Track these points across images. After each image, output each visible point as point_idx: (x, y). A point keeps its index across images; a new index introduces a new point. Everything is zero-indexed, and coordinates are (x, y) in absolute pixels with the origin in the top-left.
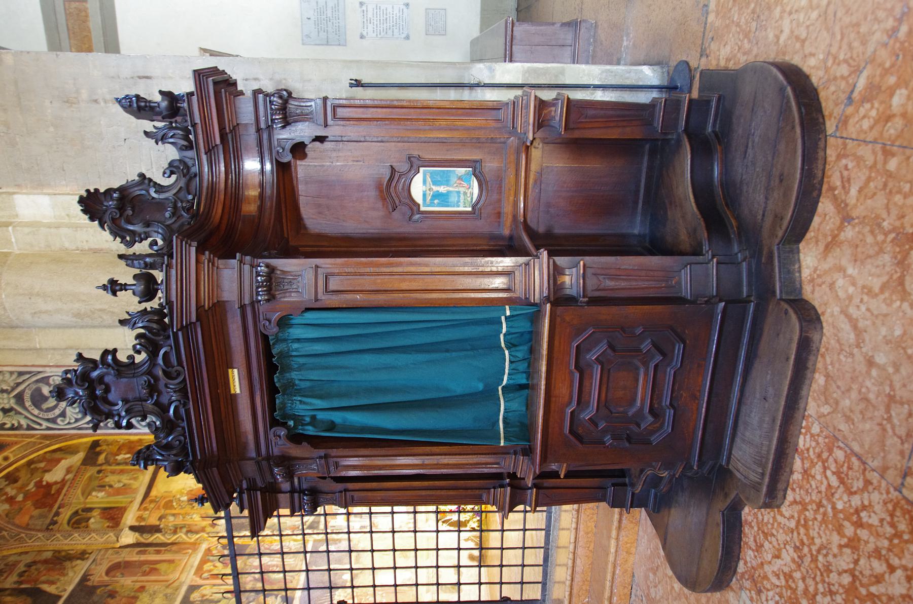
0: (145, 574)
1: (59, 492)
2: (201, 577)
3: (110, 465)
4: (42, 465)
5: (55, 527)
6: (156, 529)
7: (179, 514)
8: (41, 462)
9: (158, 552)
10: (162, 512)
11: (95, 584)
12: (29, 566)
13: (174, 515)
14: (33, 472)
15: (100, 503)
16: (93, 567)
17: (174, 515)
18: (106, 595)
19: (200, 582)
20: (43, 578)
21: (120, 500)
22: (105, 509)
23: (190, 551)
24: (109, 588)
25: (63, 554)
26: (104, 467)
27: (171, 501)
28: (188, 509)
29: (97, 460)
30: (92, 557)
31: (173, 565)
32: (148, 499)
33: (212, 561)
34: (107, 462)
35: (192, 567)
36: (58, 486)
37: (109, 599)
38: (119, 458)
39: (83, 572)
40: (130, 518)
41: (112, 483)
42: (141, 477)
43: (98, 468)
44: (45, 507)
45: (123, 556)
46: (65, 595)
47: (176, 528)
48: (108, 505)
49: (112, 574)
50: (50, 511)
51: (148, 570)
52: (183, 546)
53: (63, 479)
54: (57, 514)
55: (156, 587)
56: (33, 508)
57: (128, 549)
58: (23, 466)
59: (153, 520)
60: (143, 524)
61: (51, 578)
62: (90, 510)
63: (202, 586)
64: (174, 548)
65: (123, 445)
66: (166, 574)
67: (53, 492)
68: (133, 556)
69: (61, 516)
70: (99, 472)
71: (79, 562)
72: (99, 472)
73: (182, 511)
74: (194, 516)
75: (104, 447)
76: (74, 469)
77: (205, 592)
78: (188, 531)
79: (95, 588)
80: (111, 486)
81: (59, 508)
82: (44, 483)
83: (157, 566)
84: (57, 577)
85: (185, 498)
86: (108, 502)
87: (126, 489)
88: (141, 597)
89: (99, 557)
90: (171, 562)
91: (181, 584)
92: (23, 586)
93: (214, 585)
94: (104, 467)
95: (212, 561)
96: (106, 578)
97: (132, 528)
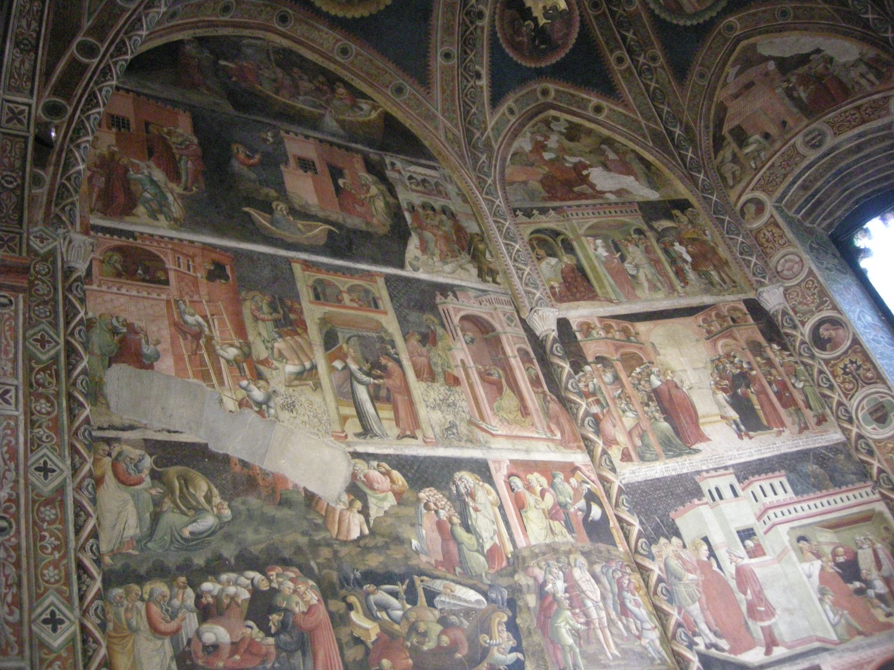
0: (484, 376)
1: (581, 196)
2: (510, 475)
3: (658, 241)
4: (612, 156)
5: (522, 218)
6: (578, 362)
7: (623, 386)
8: (616, 152)
9: (535, 382)
10: (615, 357)
11: (440, 308)
12: (444, 210)
13: (617, 378)
14: (597, 151)
15: (587, 257)
16: (472, 294)
17: (617, 378)
18: (423, 330)
19: (500, 478)
20: (428, 235)
21: (605, 281)
22: (580, 269)
23: (559, 436)
24: (440, 331)
25: (481, 246)
26: (649, 234)
27: (640, 362)
28: (638, 397)
29: (657, 219)
30: (489, 287)
32: (626, 324)
33: (552, 485)
34: (660, 236)
35: (527, 451)
36: (590, 191)
37: (418, 337)
38: (678, 247)
39: (457, 282)
40: (578, 313)
41: (629, 259)
42: (660, 295)
43: (645, 227)
44: (548, 192)
45: (508, 329)
46: (407, 273)
47: (594, 394)
48: (588, 270)
49: (467, 325)
50: (545, 199)
51: (495, 377)
52: (563, 420)
53: (604, 192)
54: (543, 211)
55: (464, 404)
56: (540, 177)
57: (523, 333)
58: (599, 136)
59: (591, 349)
60: (579, 336)
61: (432, 245)
62: (569, 248)
63: (492, 483)
64: (554, 407)
65: (704, 243)
66: (496, 412)
67: (576, 189)
68: (512, 343)
69: (543, 218)
70: (639, 232)
71: (474, 272)
72: (639, 232)
73: (629, 389)
74: (630, 414)
75: (684, 219)
76: (629, 198)
77: (480, 495)
78: (595, 417)
79: (434, 308)
80: (623, 258)
81: (554, 209)
82: (585, 173)
83: (507, 390)
84: (437, 252)
85: (656, 382)
86: (594, 269)
87: (628, 283)
88: (436, 385)
89: (493, 296)
90: (524, 411)
91: (485, 445)
92: (407, 216)
93: (501, 507)
94: (649, 234)
95: (552, 485)
96: (456, 320)
97: (563, 324)
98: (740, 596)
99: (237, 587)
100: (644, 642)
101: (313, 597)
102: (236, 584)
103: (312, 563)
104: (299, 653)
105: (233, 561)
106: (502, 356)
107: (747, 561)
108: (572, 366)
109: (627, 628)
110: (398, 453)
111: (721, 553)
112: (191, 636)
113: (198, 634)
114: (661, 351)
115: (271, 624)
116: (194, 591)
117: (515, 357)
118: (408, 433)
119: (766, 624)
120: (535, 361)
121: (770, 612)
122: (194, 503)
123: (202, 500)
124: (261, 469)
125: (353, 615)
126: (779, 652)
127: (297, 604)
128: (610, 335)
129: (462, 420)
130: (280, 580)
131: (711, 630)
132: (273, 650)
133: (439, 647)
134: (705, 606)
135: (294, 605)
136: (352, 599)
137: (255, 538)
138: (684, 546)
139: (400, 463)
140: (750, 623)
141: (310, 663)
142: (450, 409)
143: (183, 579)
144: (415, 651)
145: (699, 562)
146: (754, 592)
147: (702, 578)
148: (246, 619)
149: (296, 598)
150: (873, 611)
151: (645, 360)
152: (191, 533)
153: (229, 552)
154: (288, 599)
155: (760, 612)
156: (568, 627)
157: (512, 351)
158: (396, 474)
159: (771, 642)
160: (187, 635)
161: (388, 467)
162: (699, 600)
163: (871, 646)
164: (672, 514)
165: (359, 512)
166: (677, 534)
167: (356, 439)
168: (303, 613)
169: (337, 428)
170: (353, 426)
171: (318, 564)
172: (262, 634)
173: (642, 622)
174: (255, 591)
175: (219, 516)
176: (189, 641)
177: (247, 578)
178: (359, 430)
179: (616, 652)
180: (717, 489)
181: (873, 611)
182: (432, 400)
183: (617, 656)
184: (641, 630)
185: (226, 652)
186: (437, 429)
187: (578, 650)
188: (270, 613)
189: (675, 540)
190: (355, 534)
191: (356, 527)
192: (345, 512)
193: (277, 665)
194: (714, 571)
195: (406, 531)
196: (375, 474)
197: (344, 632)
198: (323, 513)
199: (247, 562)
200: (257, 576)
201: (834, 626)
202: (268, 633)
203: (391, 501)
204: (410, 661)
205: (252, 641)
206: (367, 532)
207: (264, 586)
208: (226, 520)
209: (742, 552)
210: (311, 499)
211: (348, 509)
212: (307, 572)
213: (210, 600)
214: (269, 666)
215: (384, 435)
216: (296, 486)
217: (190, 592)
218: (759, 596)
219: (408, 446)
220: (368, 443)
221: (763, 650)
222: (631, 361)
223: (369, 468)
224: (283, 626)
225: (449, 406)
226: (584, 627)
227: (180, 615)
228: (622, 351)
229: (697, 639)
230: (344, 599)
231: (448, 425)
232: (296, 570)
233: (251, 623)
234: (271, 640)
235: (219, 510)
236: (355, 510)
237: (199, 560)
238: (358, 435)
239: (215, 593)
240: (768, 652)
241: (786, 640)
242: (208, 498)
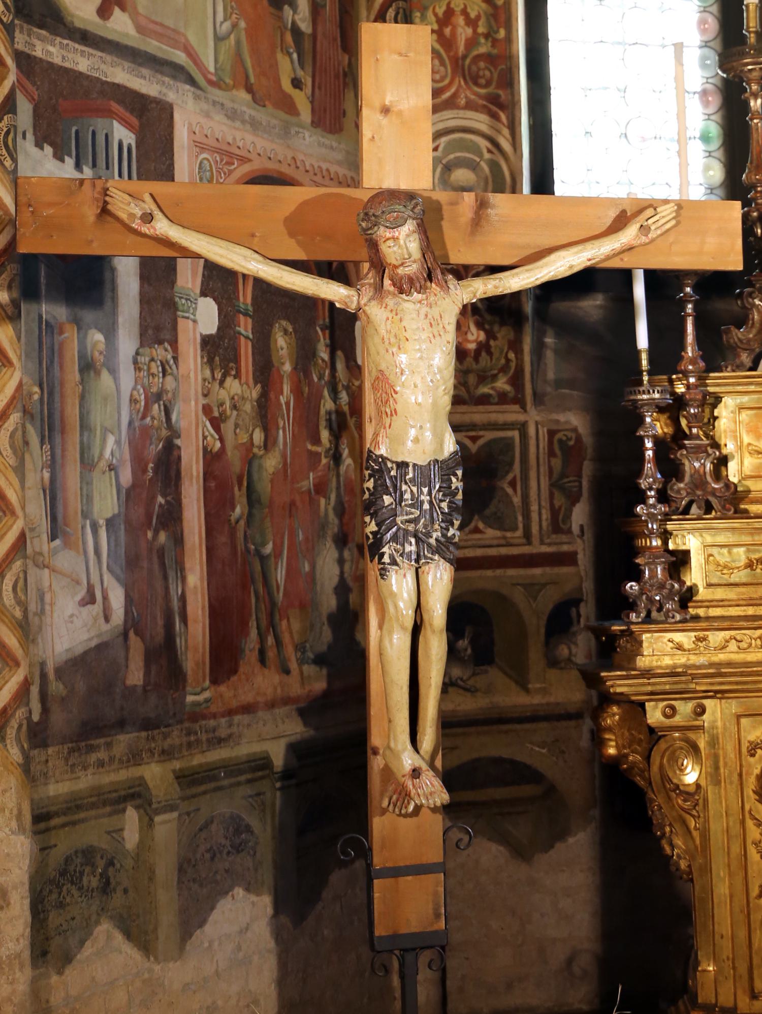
150: (279, 56)
163: (255, 125)
181: (279, 56)
201: (218, 39)
241: (141, 10)
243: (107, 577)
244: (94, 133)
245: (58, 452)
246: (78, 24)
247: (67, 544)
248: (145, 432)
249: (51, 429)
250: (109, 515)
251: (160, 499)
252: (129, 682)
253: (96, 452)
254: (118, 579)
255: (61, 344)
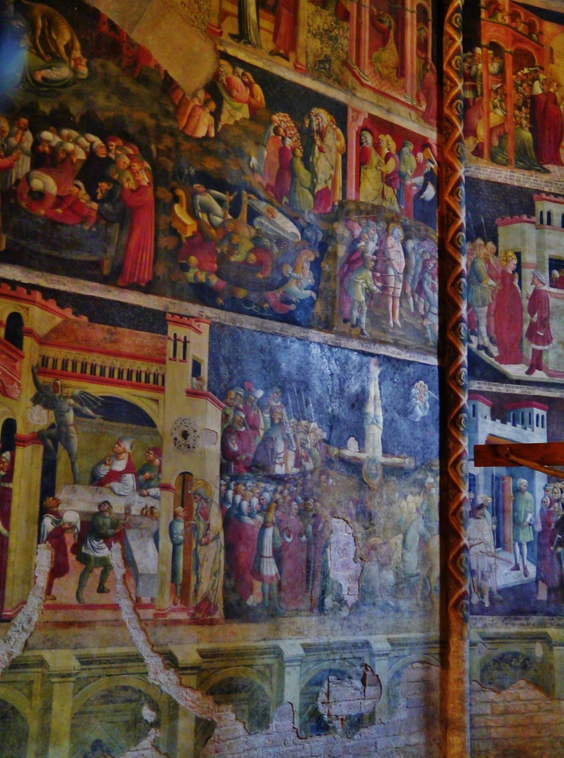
0: (375, 20)
7: (504, 82)
9: (422, 46)
13: (502, 71)
19: (353, 127)
23: (423, 108)
27: (531, 63)
28: (515, 97)
31: (394, 75)
32: (535, 19)
33: (399, 151)
35: (389, 111)
59: (490, 32)
63: (345, 131)
73: (509, 87)
74: (499, 112)
77: (330, 139)
83: (391, 44)
85: (538, 89)
88: (326, 13)
90: (401, 70)
91: (351, 91)
93: (345, 157)
95: (399, 151)
98: (527, 316)
99: (78, 146)
100: (426, 323)
101: (145, 179)
102: (76, 142)
103: (153, 147)
104: (117, 226)
105: (78, 119)
106: (399, 6)
107: (546, 288)
108: (464, 43)
109: (416, 305)
110: (266, 68)
111: (527, 273)
112: (20, 177)
113: (28, 178)
114: (557, 60)
115: (99, 190)
116: (34, 135)
117: (412, 12)
118: (282, 52)
119: (540, 348)
120: (430, 23)
121: (547, 340)
122: (53, 49)
123: (62, 49)
124: (128, 37)
125: (176, 207)
126: (539, 375)
127: (128, 180)
128: (514, 25)
129: (338, 58)
130: (119, 152)
131: (488, 335)
132: (94, 214)
133: (245, 262)
134: (492, 313)
135: (125, 180)
136: (181, 193)
137: (105, 104)
138: (496, 254)
139: (265, 78)
140: (525, 341)
141: (124, 239)
142: (330, 42)
143: (24, 121)
144: (223, 259)
145: (504, 272)
146: (540, 317)
147: (501, 288)
148: (78, 178)
149: (128, 175)
151: (537, 64)
152: (44, 78)
153: (76, 108)
154: (121, 172)
155: (539, 336)
156: (365, 285)
157: (412, 5)
158: (257, 88)
159: (536, 363)
160: (17, 174)
161: (252, 79)
162: (490, 305)
164: (498, 221)
165: (211, 113)
166: (495, 242)
167: (229, 40)
168: (132, 190)
169: (214, 21)
170: (230, 26)
171: (158, 149)
172: (87, 197)
173: (431, 305)
174: (91, 154)
175: (75, 71)
176: (18, 181)
177: (88, 141)
178: (236, 32)
179: (398, 322)
180: (549, 214)
182: (316, 27)
183: (398, 326)
184: (428, 311)
185: (50, 202)
186: (311, 59)
187: (366, 308)
188: (101, 181)
189: (490, 244)
190: (201, 133)
191: (203, 127)
192: (197, 109)
193: (94, 229)
194: (514, 287)
195: (249, 147)
196: (237, 81)
197: (164, 219)
198: (177, 102)
199: (88, 124)
200: (98, 141)
202: (94, 198)
203: (244, 113)
204: (216, 266)
205: (77, 201)
206: (213, 134)
207: (102, 154)
208: (81, 77)
209: (545, 277)
210: (169, 85)
211: (201, 107)
212: (145, 154)
213: (47, 149)
214: (86, 228)
215: (257, 46)
216: (158, 66)
217: (29, 136)
218: (544, 323)
219: (278, 64)
220: (240, 48)
221: (526, 368)
222: (522, 59)
223: (234, 72)
224: (110, 197)
225: (330, 38)
226: (378, 291)
227: (14, 154)
228: (519, 45)
229: (473, 338)
230: (173, 190)
231: (322, 58)
232: (136, 148)
233: (80, 184)
234: (95, 205)
235: (76, 65)
236: (208, 110)
237: (45, 108)
238: (232, 36)
239: (54, 144)
240: (530, 372)
241: (550, 368)
242: (69, 48)
243: (526, 562)
244: (523, 414)
245: (501, 519)
246: (514, 378)
247: (505, 549)
248: (550, 513)
249: (497, 512)
250: (529, 540)
251: (559, 536)
252: (539, 598)
253: (522, 519)
254: (533, 563)
255: (503, 485)
